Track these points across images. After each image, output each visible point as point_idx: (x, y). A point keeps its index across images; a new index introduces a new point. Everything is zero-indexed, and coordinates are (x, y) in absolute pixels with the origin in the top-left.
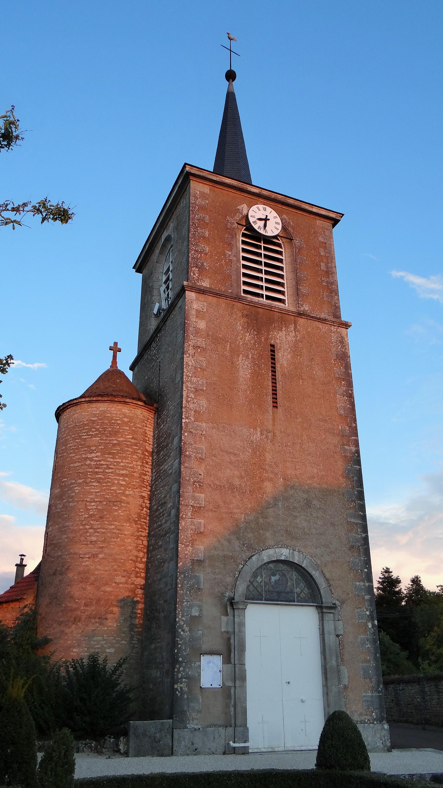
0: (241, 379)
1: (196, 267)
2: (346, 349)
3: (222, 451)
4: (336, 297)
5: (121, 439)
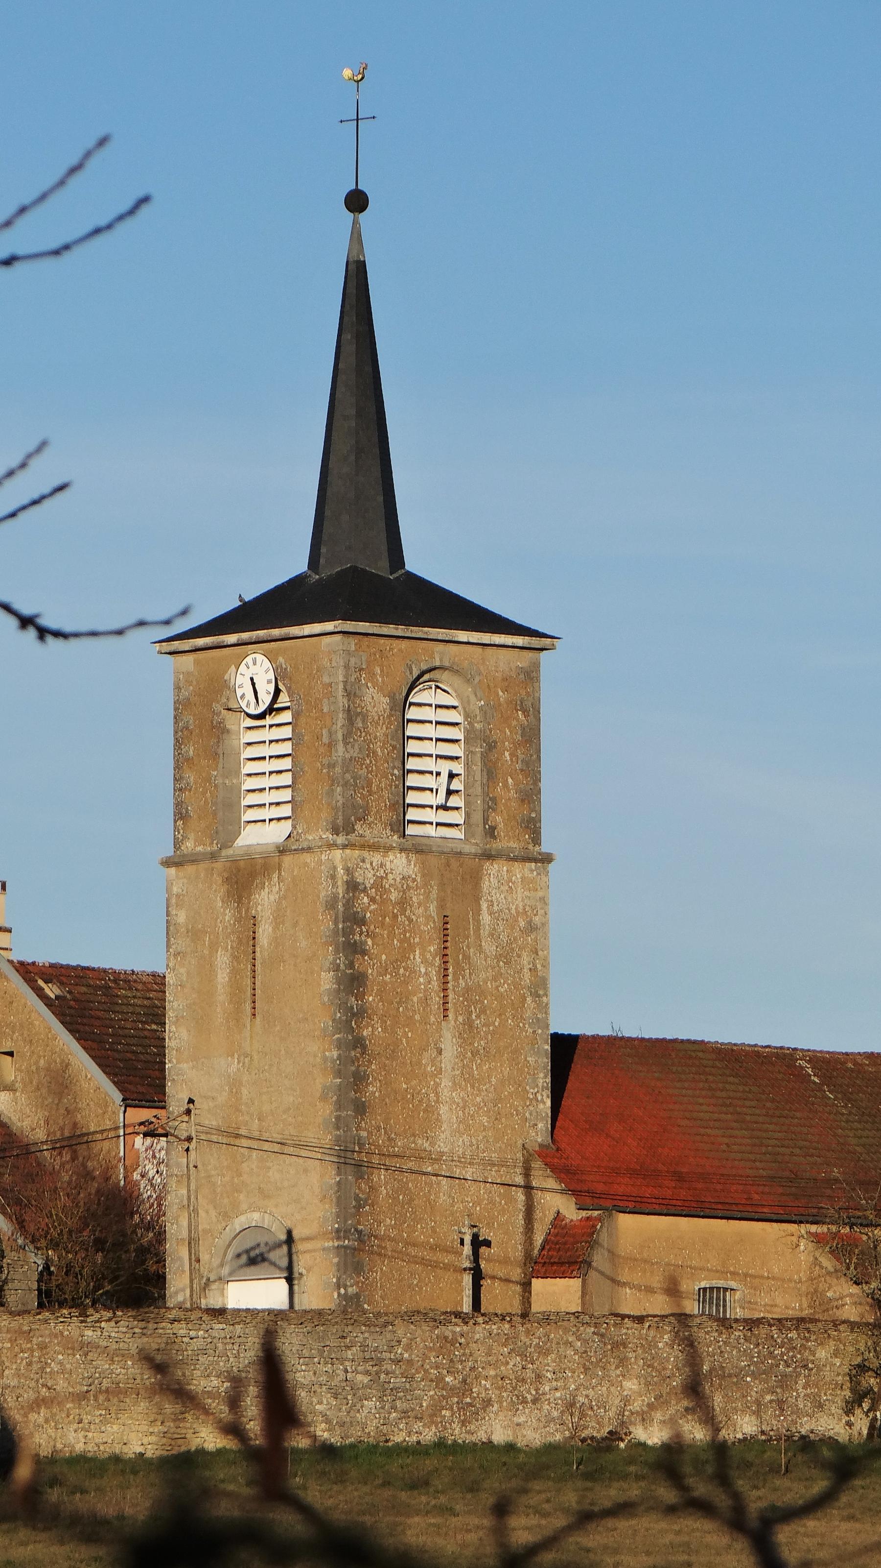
0: (219, 987)
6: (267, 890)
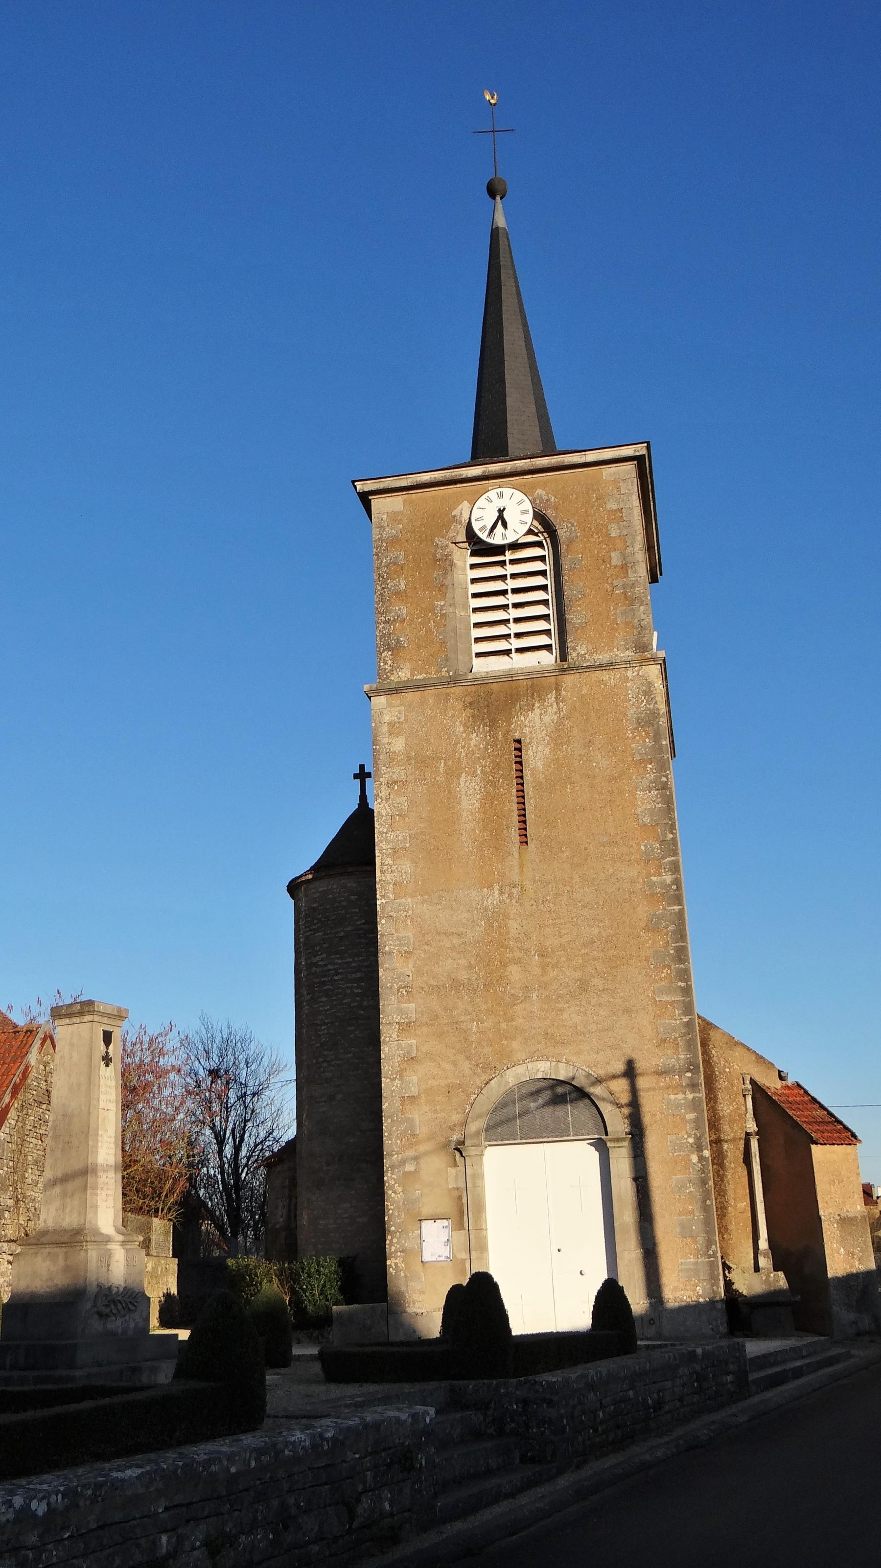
0: (465, 814)
1: (388, 649)
2: (656, 703)
3: (438, 933)
5: (349, 928)
6: (537, 711)
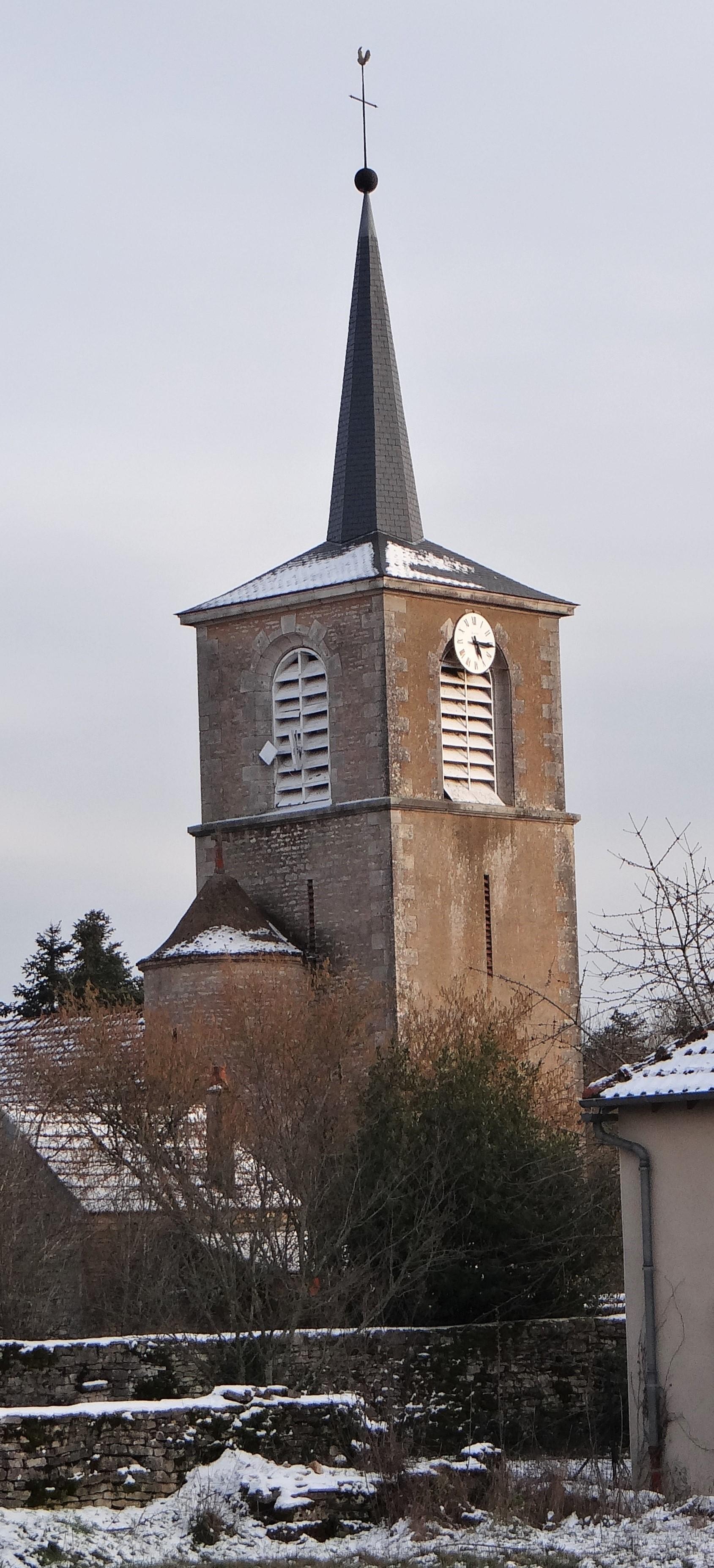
0: (454, 940)
1: (397, 761)
4: (560, 765)
6: (499, 850)
